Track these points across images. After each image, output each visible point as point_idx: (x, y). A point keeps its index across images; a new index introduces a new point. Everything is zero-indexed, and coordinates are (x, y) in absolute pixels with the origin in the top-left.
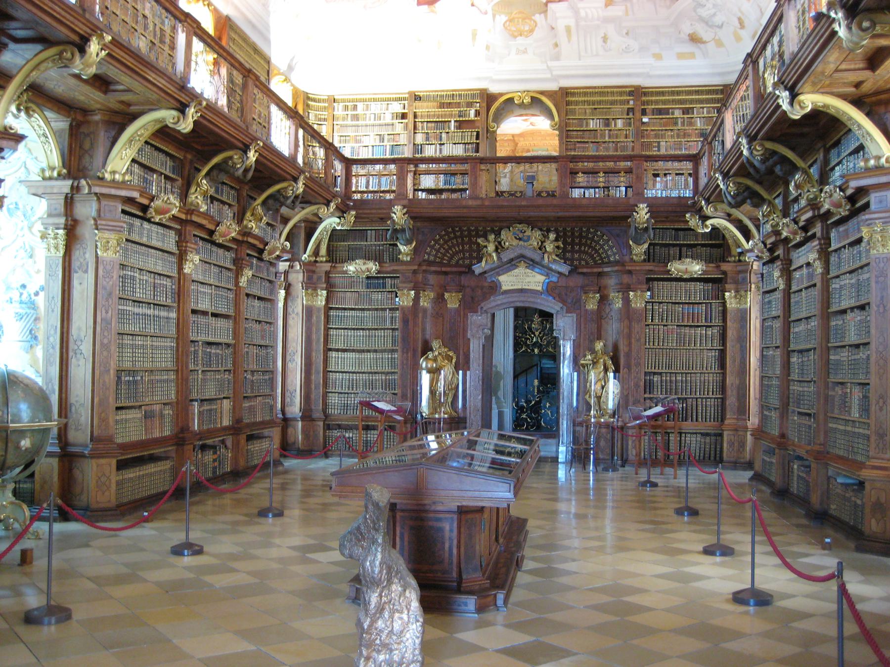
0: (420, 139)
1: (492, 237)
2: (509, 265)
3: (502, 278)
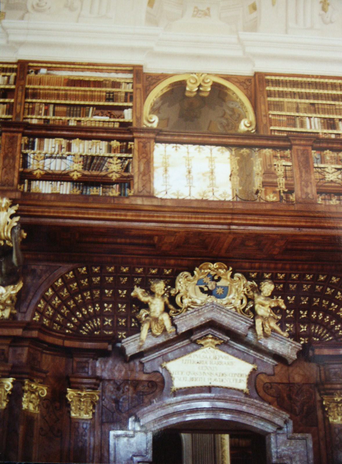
1: (159, 287)
2: (186, 342)
3: (172, 366)
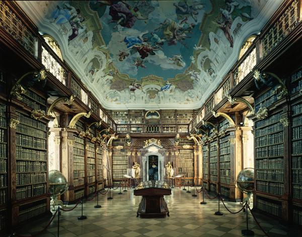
0: (131, 120)
